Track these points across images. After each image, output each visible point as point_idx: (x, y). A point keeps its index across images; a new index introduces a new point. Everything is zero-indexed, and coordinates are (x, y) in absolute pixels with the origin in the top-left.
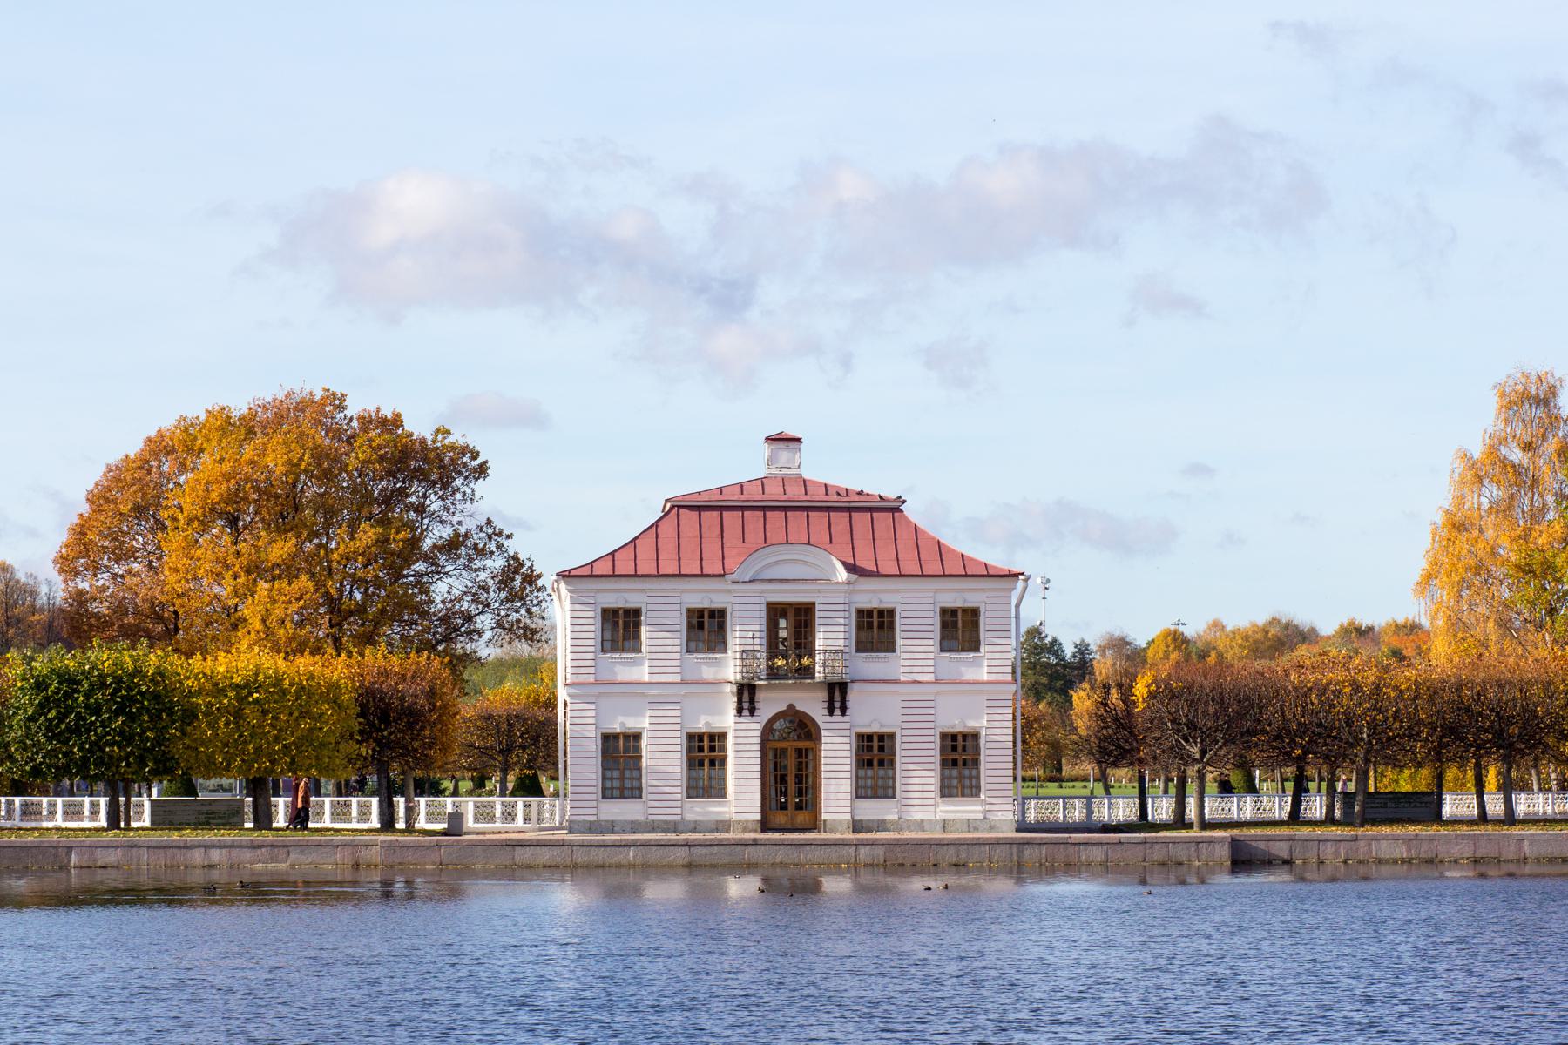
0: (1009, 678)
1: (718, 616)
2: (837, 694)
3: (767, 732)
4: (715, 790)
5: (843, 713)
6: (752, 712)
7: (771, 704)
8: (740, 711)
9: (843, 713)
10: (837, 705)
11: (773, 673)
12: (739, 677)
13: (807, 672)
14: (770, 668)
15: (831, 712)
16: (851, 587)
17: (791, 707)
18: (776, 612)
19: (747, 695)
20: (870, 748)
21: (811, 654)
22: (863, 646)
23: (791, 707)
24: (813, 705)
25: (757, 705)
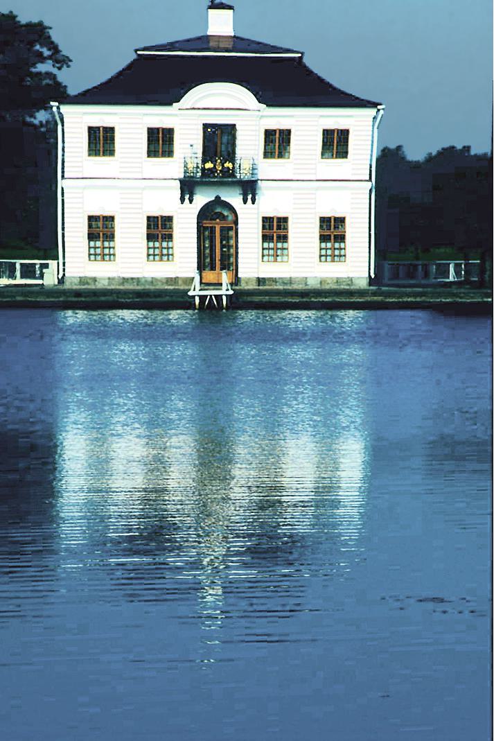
0: (368, 178)
2: (249, 188)
4: (166, 256)
5: (253, 203)
6: (191, 201)
7: (202, 198)
8: (182, 200)
9: (253, 203)
10: (250, 197)
12: (182, 176)
14: (203, 169)
15: (245, 201)
16: (260, 113)
17: (218, 198)
19: (188, 187)
20: (271, 228)
21: (233, 160)
22: (268, 154)
23: (218, 198)
24: (233, 198)
25: (195, 197)
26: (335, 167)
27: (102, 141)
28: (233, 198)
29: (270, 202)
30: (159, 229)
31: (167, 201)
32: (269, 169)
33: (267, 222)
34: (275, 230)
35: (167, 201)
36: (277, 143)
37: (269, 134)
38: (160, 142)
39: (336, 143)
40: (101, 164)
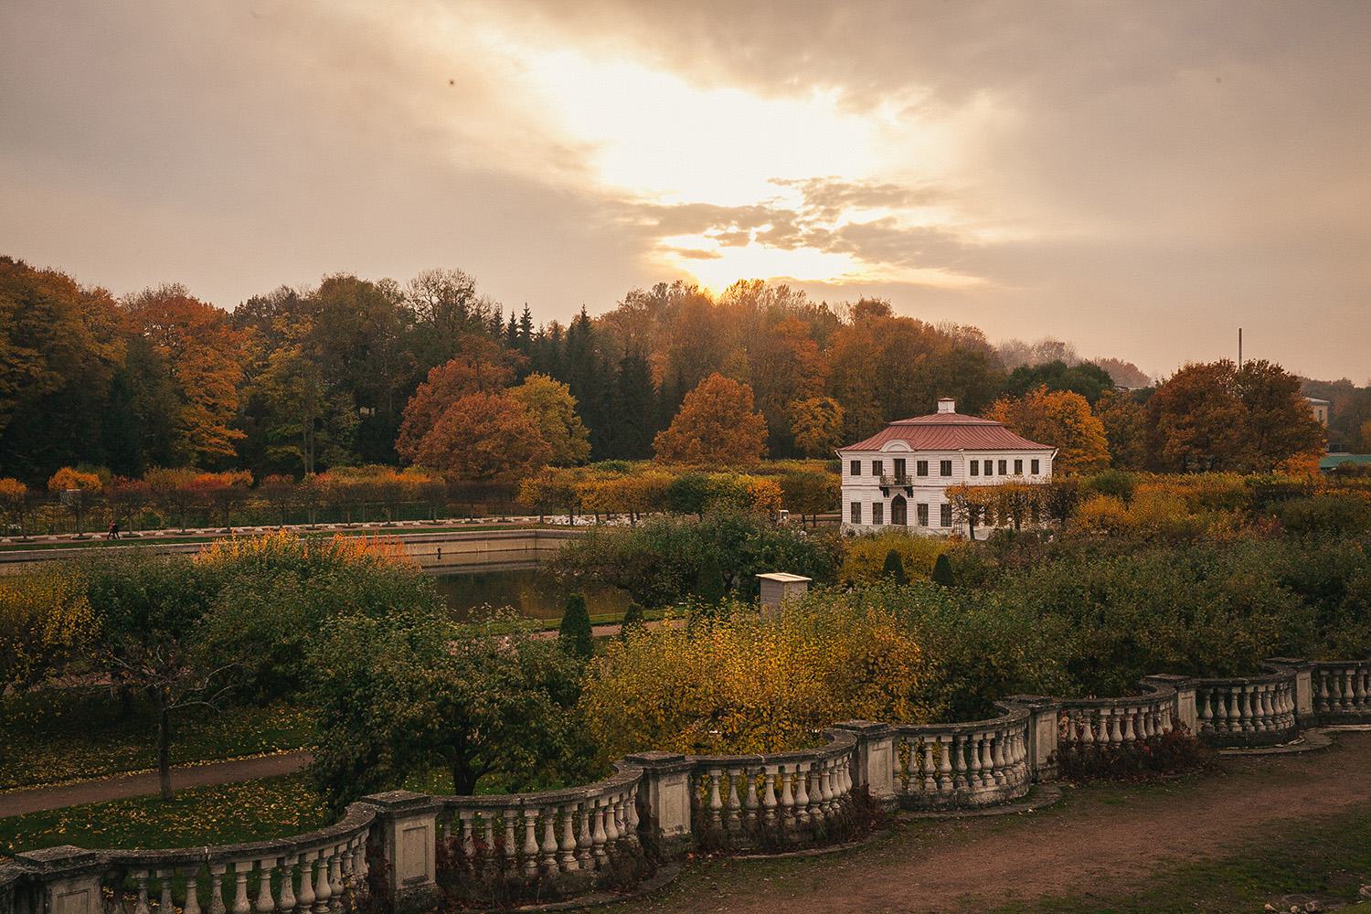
2: (910, 492)
11: (897, 483)
13: (903, 483)
19: (885, 490)
24: (904, 495)
28: (904, 495)
29: (919, 497)
30: (877, 508)
34: (923, 510)
35: (878, 496)
36: (923, 469)
38: (877, 468)
39: (946, 469)
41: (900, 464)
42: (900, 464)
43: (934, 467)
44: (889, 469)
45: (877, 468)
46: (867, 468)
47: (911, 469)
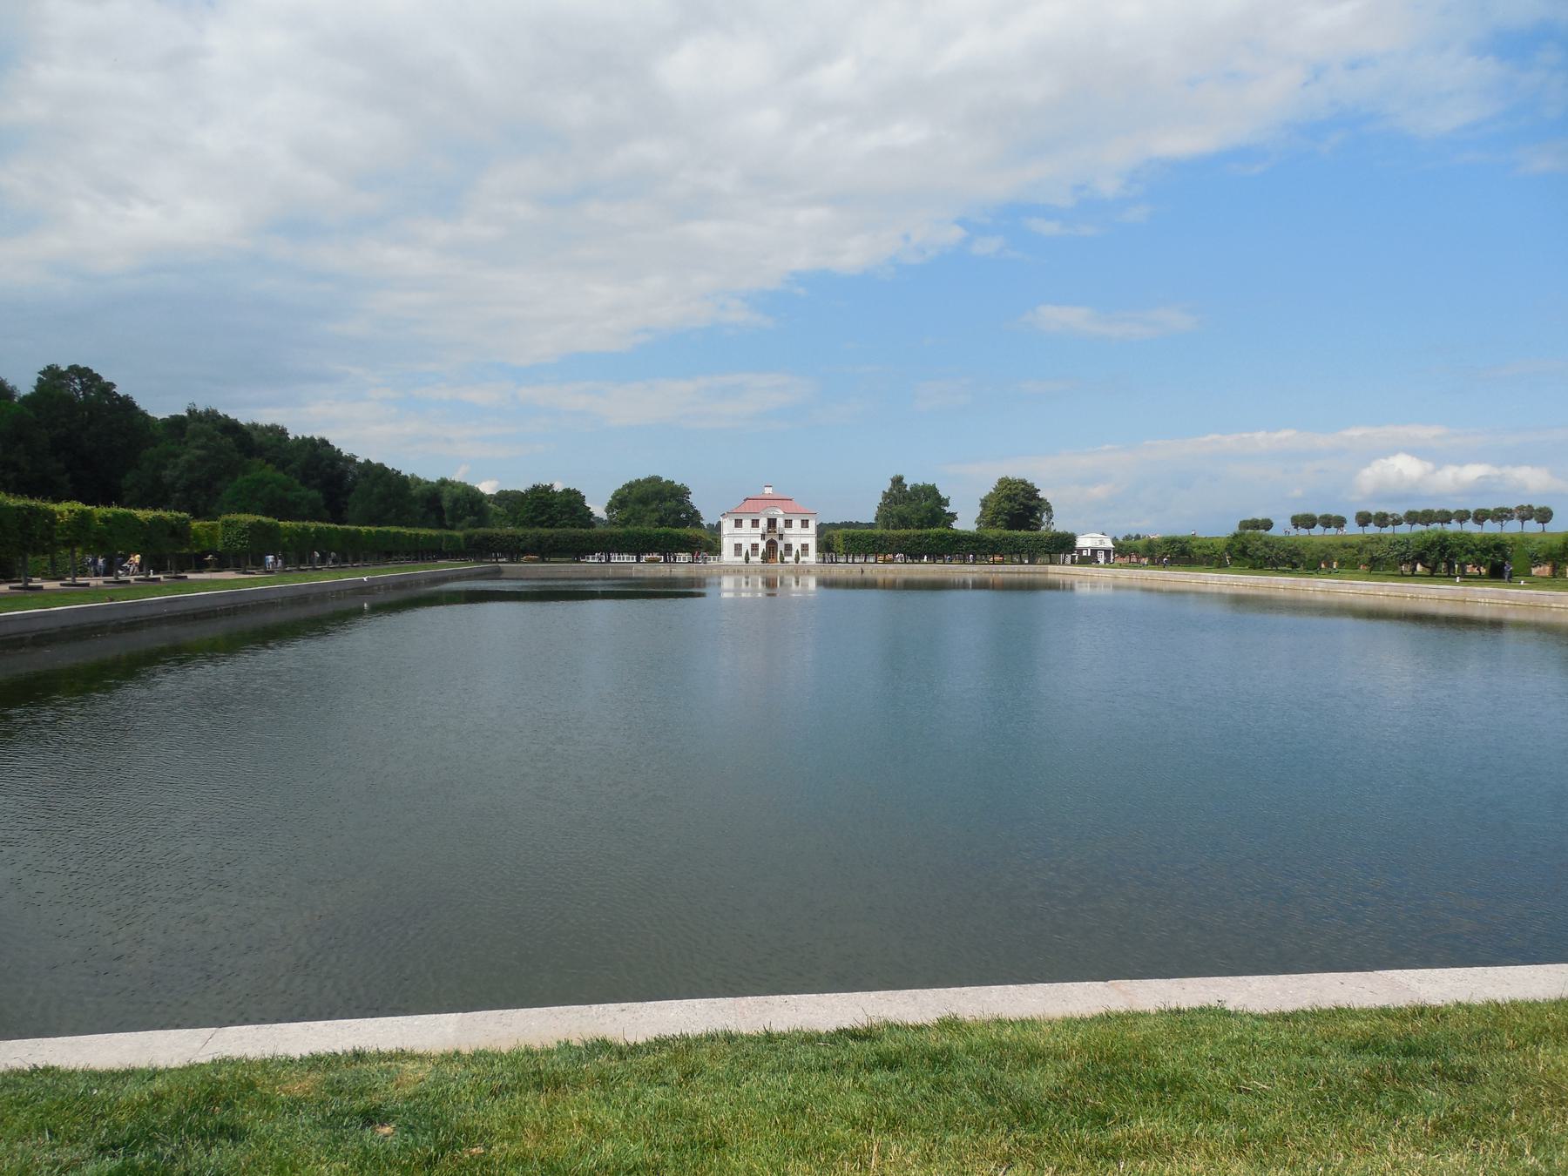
1: (758, 521)
2: (781, 536)
3: (768, 543)
7: (767, 539)
11: (769, 532)
13: (775, 532)
18: (769, 520)
19: (763, 537)
24: (776, 539)
26: (804, 531)
27: (738, 523)
31: (758, 540)
32: (787, 531)
33: (786, 545)
34: (788, 547)
35: (758, 540)
36: (788, 523)
37: (786, 521)
38: (755, 523)
39: (805, 524)
40: (738, 531)
41: (772, 523)
42: (772, 523)
43: (797, 523)
44: (763, 523)
45: (755, 523)
46: (747, 523)
47: (780, 523)
